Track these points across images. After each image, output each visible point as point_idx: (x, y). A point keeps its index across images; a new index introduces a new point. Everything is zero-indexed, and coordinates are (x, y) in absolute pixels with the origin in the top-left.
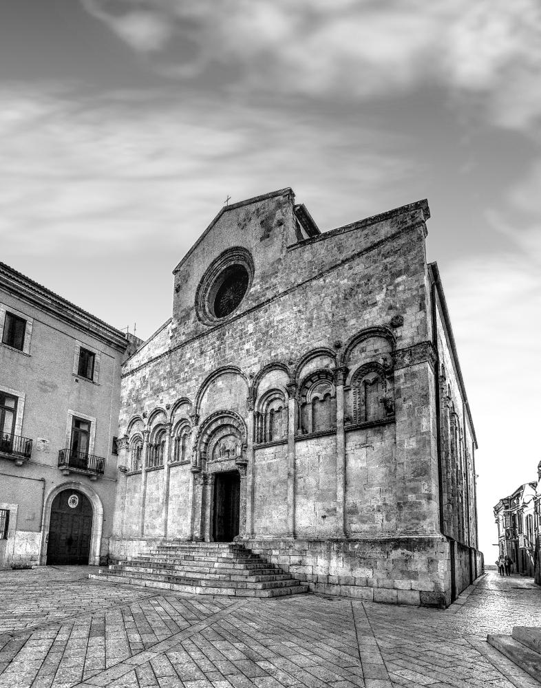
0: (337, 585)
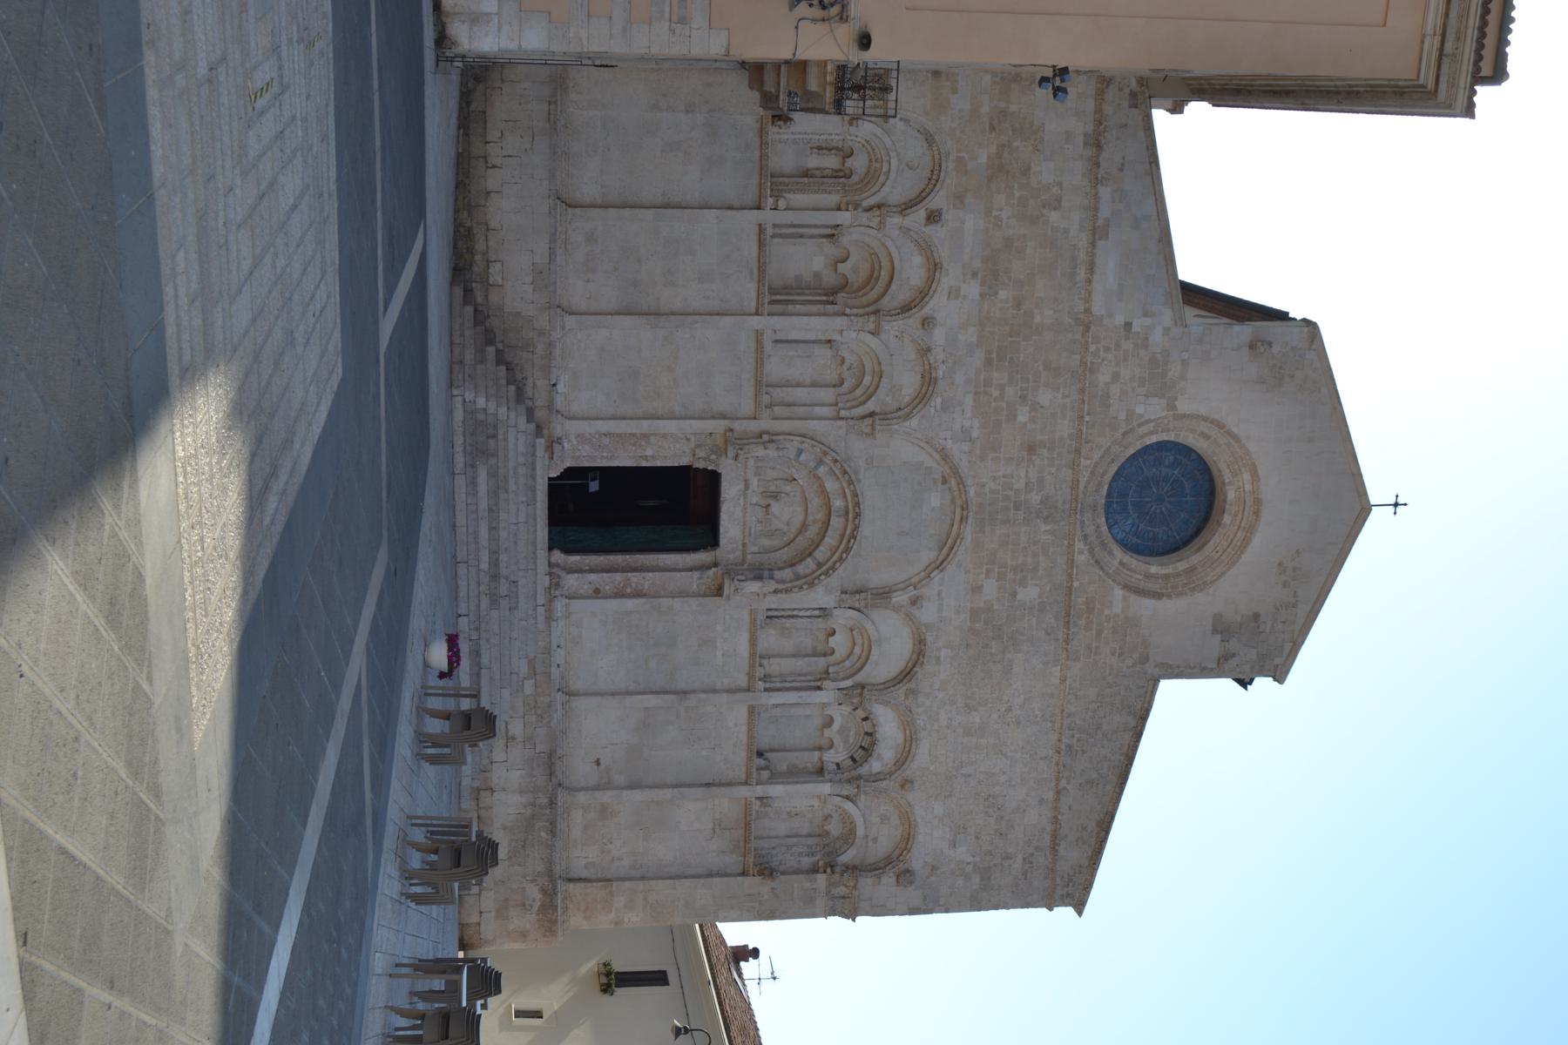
0: (478, 805)
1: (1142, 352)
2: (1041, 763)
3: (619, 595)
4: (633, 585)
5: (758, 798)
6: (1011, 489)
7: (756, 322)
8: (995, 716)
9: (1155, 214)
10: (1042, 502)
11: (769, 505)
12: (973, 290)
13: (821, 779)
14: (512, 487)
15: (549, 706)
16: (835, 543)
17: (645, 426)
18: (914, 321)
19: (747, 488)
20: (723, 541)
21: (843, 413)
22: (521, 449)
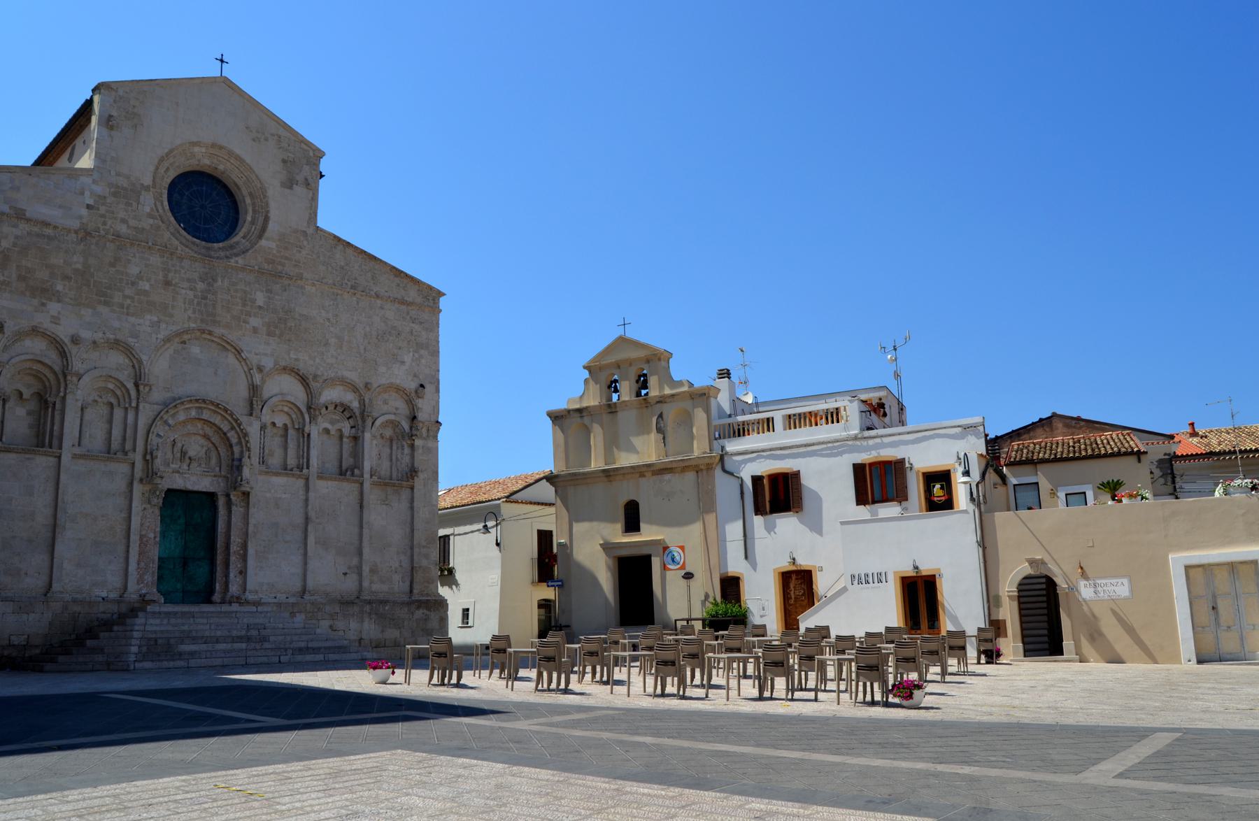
1: (108, 201)
2: (360, 305)
3: (244, 558)
4: (238, 549)
5: (371, 477)
6: (193, 300)
7: (65, 458)
8: (332, 329)
9: (9, 174)
10: (203, 282)
11: (190, 458)
12: (54, 307)
13: (361, 438)
14: (186, 628)
15: (313, 604)
16: (219, 417)
17: (134, 538)
18: (72, 349)
19: (178, 472)
20: (212, 490)
21: (134, 404)
22: (158, 621)
